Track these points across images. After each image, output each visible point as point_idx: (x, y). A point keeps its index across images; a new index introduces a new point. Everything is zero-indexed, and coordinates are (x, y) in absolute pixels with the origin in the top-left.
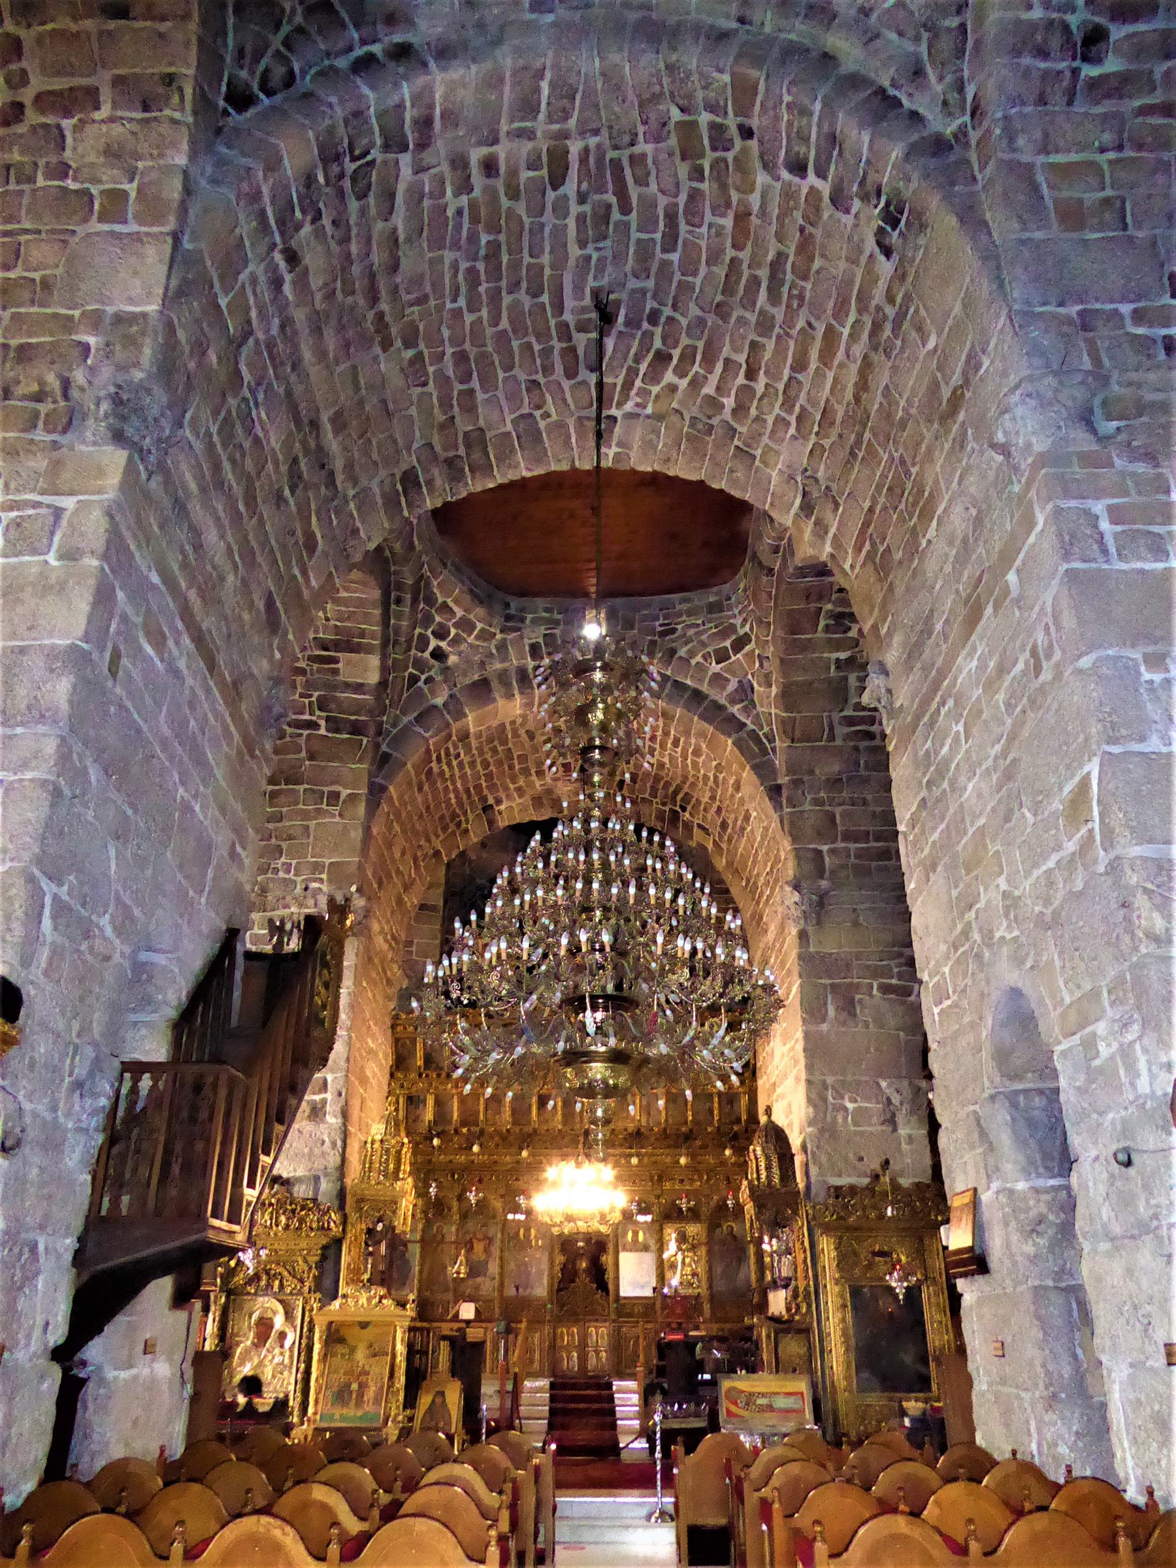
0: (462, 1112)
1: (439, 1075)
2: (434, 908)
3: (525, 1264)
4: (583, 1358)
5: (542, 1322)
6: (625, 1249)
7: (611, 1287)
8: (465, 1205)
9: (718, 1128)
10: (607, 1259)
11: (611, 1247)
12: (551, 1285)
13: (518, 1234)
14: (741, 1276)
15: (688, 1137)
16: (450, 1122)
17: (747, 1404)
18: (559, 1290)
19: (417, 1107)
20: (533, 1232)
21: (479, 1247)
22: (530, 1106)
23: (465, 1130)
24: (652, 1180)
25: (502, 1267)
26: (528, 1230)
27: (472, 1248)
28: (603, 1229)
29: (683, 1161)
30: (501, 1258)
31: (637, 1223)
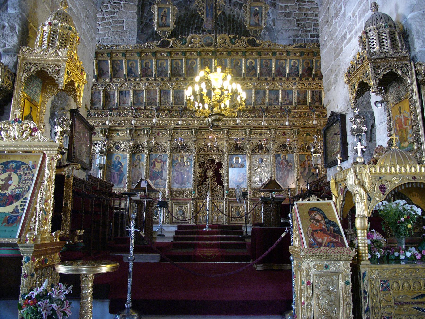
1: (135, 80)
6: (232, 166)
7: (225, 184)
8: (151, 145)
10: (223, 171)
11: (225, 164)
13: (178, 160)
15: (267, 110)
16: (142, 103)
18: (198, 185)
19: (125, 96)
20: (185, 158)
21: (158, 165)
23: (149, 107)
25: (169, 175)
27: (155, 166)
30: (169, 171)
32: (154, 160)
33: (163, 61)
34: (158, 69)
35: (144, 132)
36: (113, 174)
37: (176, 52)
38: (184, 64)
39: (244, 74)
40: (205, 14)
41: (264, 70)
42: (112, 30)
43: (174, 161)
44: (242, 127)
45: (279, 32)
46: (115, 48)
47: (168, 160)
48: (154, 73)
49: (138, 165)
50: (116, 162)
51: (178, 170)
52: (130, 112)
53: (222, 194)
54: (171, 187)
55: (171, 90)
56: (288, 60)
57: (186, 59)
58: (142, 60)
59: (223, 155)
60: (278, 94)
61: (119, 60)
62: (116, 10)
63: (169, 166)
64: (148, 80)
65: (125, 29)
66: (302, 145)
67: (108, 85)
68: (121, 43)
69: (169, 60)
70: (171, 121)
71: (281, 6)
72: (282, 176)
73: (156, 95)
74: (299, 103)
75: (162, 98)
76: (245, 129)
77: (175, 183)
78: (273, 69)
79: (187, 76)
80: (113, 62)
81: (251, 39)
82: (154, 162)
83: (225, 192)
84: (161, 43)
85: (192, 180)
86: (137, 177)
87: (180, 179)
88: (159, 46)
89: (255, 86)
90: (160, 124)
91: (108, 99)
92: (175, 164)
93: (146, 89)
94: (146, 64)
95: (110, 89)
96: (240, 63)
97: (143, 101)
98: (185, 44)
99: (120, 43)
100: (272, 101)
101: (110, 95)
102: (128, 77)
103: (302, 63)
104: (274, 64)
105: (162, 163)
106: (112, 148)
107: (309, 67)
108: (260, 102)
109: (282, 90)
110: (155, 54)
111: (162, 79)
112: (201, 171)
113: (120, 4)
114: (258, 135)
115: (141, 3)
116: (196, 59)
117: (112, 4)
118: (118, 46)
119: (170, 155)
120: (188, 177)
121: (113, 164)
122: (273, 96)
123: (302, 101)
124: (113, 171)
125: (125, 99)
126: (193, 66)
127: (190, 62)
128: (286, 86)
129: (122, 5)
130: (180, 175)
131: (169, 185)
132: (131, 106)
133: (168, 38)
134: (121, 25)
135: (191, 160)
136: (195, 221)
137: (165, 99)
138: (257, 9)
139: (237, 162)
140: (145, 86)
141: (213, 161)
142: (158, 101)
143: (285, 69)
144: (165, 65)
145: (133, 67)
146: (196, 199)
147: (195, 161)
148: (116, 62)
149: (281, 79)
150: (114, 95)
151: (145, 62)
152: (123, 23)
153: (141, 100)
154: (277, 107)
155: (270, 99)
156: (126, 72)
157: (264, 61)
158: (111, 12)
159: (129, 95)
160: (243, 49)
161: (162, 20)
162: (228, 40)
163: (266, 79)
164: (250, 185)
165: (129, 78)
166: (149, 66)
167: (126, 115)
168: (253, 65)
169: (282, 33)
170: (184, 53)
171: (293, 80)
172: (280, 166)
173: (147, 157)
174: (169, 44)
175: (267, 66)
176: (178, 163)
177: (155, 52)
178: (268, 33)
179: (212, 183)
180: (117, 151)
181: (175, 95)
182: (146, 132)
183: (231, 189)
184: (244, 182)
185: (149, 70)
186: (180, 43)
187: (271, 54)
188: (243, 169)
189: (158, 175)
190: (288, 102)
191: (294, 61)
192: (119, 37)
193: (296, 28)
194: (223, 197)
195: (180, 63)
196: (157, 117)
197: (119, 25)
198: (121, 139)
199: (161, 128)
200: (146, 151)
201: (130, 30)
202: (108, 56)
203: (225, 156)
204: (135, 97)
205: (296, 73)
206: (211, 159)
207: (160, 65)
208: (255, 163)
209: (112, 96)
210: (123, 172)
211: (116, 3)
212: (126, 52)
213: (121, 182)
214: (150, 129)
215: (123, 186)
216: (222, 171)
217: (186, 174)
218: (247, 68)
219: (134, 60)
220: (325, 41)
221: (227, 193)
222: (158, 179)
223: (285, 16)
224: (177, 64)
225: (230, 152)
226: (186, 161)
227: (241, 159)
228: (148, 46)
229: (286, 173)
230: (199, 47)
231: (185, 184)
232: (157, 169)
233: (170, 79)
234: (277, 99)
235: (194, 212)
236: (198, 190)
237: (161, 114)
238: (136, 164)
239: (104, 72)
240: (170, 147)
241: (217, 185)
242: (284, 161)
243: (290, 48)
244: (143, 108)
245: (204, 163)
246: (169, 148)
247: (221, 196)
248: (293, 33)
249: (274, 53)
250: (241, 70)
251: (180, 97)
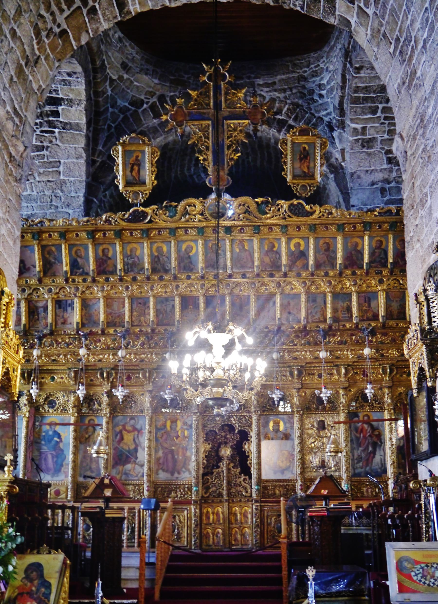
0: (107, 314)
1: (84, 280)
2: (77, 127)
3: (172, 452)
4: (228, 533)
5: (189, 503)
6: (267, 437)
7: (254, 472)
9: (357, 325)
12: (197, 471)
13: (165, 425)
14: (377, 458)
16: (96, 323)
17: (424, 576)
18: (204, 475)
19: (65, 310)
20: (179, 424)
21: (128, 438)
22: (173, 306)
23: (111, 331)
24: (292, 374)
25: (150, 455)
26: (174, 422)
27: (122, 438)
28: (244, 395)
29: (322, 355)
30: (149, 448)
31: (279, 413)
32: (121, 427)
33: (135, 245)
34: (126, 260)
35: (102, 375)
36: (43, 456)
37: (159, 230)
38: (173, 249)
39: (285, 266)
40: (210, 159)
41: (322, 258)
42: (38, 179)
43: (158, 429)
44: (285, 363)
45: (352, 175)
46: (47, 223)
47: (147, 427)
48: (119, 267)
49: (92, 437)
50: (51, 433)
51: (166, 445)
52: (75, 339)
53: (249, 491)
54: (153, 478)
55: (151, 299)
56: (366, 238)
57: (178, 241)
58: (96, 243)
59: (251, 417)
60: (350, 301)
61: (53, 245)
62: (46, 144)
63: (149, 440)
64: (107, 280)
65: (62, 177)
66: (400, 394)
67: (34, 290)
68: (56, 202)
69: (145, 244)
70: (152, 354)
71: (355, 129)
72: (363, 455)
73: (124, 307)
74: (389, 315)
75: (135, 313)
76: (289, 367)
77: (160, 472)
78: (339, 255)
79: (179, 273)
80: (43, 248)
81: (295, 203)
82: (121, 432)
83: (255, 487)
84: (130, 214)
85: (192, 465)
86: (89, 460)
87: (170, 464)
88: (128, 220)
89: (306, 287)
90: (131, 360)
91: (34, 316)
92: (159, 434)
93: (104, 297)
94: (103, 251)
95: (38, 296)
96: (276, 245)
97: (99, 319)
98: (175, 216)
99: (54, 203)
100: (340, 315)
101: (37, 308)
102: (71, 274)
103: (394, 242)
104: (340, 246)
105: (136, 433)
106: (42, 406)
108: (318, 316)
109: (358, 293)
110: (119, 234)
111: (134, 279)
112: (208, 447)
113: (54, 132)
114: (316, 377)
115: (91, 129)
116: (196, 241)
117: (38, 132)
118: (53, 220)
119: (151, 418)
120: (185, 461)
121: (44, 436)
122: (341, 305)
123: (395, 313)
124: (45, 449)
125: (65, 317)
126: (191, 254)
127: (184, 246)
128: (364, 285)
129: (57, 134)
130: (170, 456)
131: (149, 476)
132: (78, 330)
133: (146, 204)
134: (54, 169)
135: (191, 426)
136: (198, 544)
137: (140, 316)
138: (305, 148)
139: (276, 430)
140: (103, 291)
141: (231, 428)
142: (127, 318)
143: (362, 255)
144: (138, 253)
145: (81, 257)
146: (201, 502)
147: (197, 428)
148: (48, 249)
149: (354, 273)
150: (46, 308)
151: (101, 248)
152: (58, 167)
153: (95, 318)
154: (348, 326)
155: (335, 310)
156: (66, 266)
157: (321, 242)
158: (37, 146)
159: (73, 309)
160: (283, 222)
161: (132, 171)
162: (253, 207)
163: (327, 274)
164: (301, 473)
165: (73, 277)
166: (110, 255)
167: (68, 344)
168: (302, 248)
169: (359, 177)
170: (173, 231)
171: (376, 273)
172: (358, 435)
173: (108, 423)
174: (146, 217)
175: (327, 250)
176: (167, 433)
177: (121, 231)
178: (332, 176)
179: (229, 470)
180: (51, 411)
181: (159, 307)
182: (105, 375)
183: (267, 481)
184: (289, 467)
185: (109, 262)
186: (165, 214)
187: (333, 229)
188: (288, 443)
189: (127, 457)
190: (370, 315)
191: (379, 238)
192: (51, 191)
193: (385, 166)
194: (251, 496)
195: (165, 249)
196: (126, 347)
197: (50, 170)
198: (59, 387)
199: (134, 367)
200: (106, 411)
201: (72, 179)
202: (33, 237)
203: (254, 418)
204: (84, 311)
205: (383, 261)
206: (228, 425)
207: (129, 253)
208: (310, 432)
209: (41, 310)
210: (62, 451)
211: (46, 132)
212: (66, 232)
213: (59, 470)
214: (112, 369)
215: (61, 477)
216: (249, 447)
217: (180, 454)
218: (290, 254)
219: (81, 245)
220: (412, 238)
221: (258, 490)
222: (129, 462)
223: (363, 147)
224: (159, 249)
225: (264, 411)
226: (182, 428)
227: (285, 423)
228: (107, 221)
229: (370, 449)
230: (200, 221)
231: (179, 473)
232: (126, 444)
233: (148, 279)
234: (349, 309)
235: (196, 526)
236: (203, 484)
237: (134, 343)
238: (87, 436)
239: (27, 267)
240: (151, 403)
241: (240, 474)
242: (366, 426)
243: (369, 218)
244: (100, 332)
245: (215, 432)
246: (148, 405)
247: (248, 495)
248: (379, 176)
249: (340, 228)
250: (280, 258)
251: (168, 309)
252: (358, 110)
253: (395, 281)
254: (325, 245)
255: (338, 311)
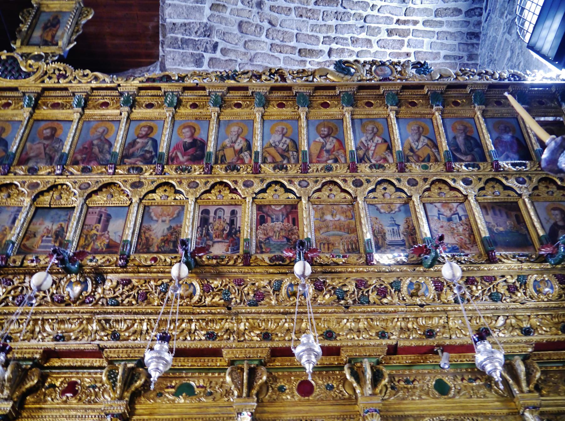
107: (195, 141)
205: (148, 155)
252: (177, 56)
253: (165, 187)
254: (48, 131)
255: (35, 236)
